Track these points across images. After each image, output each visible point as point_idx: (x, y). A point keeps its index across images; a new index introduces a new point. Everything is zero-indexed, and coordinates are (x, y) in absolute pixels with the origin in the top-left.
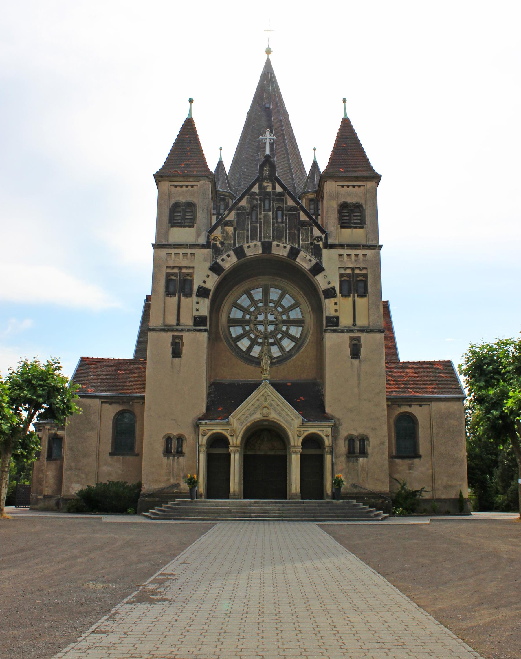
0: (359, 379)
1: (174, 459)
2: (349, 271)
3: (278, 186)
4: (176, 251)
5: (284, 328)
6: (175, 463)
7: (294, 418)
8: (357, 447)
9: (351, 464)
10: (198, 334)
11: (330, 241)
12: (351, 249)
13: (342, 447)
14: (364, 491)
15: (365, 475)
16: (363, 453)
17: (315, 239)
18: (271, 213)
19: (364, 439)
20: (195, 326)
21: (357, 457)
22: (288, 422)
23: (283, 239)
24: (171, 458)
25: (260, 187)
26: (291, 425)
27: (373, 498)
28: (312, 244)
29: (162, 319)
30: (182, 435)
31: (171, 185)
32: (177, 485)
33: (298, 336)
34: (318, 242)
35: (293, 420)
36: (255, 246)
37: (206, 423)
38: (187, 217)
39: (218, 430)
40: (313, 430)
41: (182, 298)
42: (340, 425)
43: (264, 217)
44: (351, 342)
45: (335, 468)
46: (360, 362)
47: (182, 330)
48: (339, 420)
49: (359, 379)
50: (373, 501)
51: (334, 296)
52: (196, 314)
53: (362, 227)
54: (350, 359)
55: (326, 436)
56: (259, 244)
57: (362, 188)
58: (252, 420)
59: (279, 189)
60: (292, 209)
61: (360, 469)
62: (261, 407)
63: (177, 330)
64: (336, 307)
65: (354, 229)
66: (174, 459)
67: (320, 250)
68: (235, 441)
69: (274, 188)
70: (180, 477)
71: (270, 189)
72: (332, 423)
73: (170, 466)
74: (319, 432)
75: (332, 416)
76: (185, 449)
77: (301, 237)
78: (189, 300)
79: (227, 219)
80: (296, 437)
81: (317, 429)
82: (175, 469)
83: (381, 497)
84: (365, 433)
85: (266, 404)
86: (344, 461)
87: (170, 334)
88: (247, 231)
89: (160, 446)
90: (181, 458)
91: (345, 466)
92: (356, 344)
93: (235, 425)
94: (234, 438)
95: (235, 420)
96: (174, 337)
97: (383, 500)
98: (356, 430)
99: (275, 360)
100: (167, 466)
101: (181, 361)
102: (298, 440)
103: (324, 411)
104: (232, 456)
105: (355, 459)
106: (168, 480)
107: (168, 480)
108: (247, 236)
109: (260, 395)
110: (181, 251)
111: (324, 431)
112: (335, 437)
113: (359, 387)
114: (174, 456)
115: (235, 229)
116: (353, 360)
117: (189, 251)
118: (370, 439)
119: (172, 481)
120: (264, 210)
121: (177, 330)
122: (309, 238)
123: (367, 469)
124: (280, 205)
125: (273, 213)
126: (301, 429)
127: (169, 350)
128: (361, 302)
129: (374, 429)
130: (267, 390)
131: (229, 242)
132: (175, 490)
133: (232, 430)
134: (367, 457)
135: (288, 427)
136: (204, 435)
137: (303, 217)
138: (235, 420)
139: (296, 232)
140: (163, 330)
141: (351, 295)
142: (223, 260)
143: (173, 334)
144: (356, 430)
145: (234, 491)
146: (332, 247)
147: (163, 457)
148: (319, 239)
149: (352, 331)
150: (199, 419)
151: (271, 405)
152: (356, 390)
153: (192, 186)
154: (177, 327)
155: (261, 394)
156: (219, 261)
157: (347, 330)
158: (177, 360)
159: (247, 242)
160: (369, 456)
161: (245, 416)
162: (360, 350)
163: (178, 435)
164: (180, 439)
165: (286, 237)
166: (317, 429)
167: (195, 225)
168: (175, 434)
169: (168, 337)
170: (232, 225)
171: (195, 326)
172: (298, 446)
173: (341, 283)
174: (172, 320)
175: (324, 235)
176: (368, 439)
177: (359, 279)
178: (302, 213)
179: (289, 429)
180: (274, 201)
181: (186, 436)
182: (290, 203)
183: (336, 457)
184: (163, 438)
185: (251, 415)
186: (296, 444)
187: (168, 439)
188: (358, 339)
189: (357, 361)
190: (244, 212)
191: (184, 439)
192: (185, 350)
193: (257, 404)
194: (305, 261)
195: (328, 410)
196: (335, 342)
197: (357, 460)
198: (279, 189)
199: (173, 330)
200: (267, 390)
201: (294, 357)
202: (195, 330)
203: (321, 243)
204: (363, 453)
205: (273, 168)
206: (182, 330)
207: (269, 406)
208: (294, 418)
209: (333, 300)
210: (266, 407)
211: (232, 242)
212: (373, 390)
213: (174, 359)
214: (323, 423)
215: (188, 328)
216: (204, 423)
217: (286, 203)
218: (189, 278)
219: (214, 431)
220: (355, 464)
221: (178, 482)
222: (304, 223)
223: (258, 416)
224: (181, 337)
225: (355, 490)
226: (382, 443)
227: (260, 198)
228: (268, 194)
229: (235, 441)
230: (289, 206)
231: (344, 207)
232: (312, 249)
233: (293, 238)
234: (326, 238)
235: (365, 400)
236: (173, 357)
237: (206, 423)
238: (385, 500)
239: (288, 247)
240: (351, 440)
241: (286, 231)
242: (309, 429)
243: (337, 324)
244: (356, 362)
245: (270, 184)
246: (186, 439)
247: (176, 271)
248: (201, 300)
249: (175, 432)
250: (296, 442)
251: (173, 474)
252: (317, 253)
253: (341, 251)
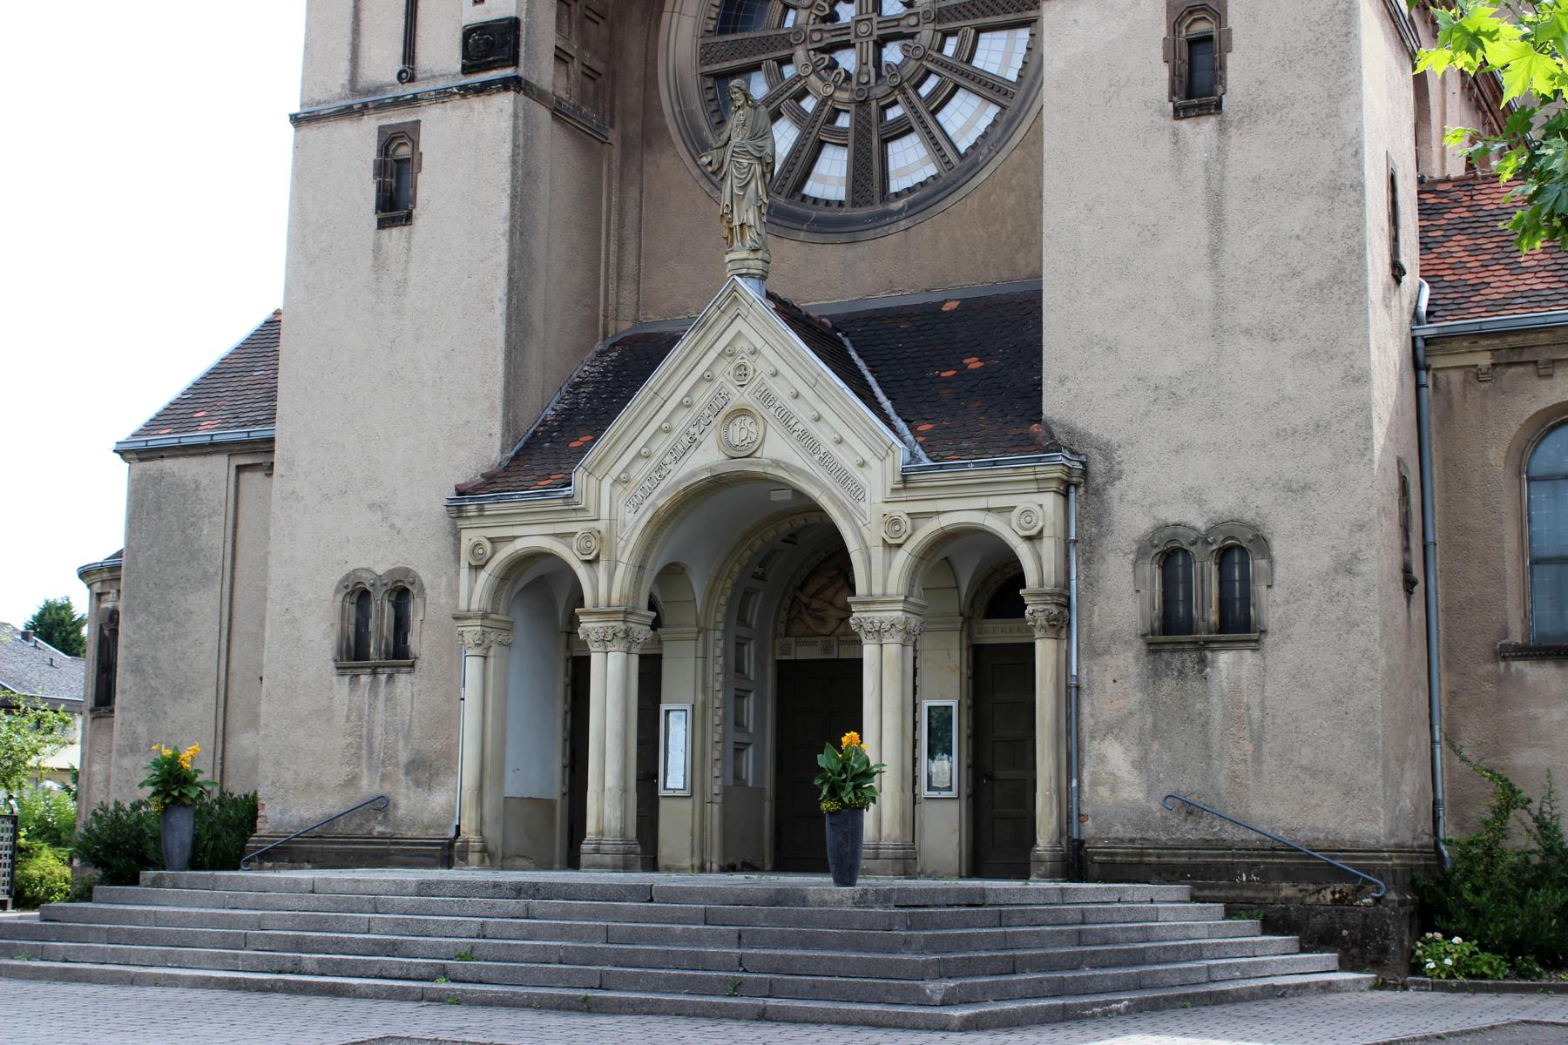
0: (1217, 220)
1: (374, 688)
6: (380, 706)
7: (867, 455)
8: (1208, 595)
9: (1168, 685)
10: (476, 103)
13: (1123, 597)
14: (1240, 835)
15: (1248, 747)
16: (1238, 624)
19: (1238, 552)
20: (466, 70)
21: (1202, 646)
22: (844, 478)
24: (365, 679)
26: (858, 492)
27: (1288, 874)
29: (344, 66)
30: (407, 571)
32: (380, 805)
33: (1012, 76)
35: (863, 464)
37: (481, 509)
39: (532, 537)
40: (960, 512)
42: (1113, 476)
44: (1175, 26)
45: (1086, 709)
46: (1222, 129)
47: (415, 100)
48: (1107, 450)
49: (1217, 220)
50: (1287, 890)
54: (1169, 122)
55: (1029, 538)
58: (679, 482)
61: (1217, 715)
62: (721, 416)
63: (398, 102)
66: (374, 688)
68: (607, 585)
70: (397, 765)
72: (1052, 470)
73: (360, 718)
74: (993, 523)
75: (1070, 432)
80: (878, 553)
81: (982, 503)
82: (378, 731)
83: (1340, 874)
84: (1249, 516)
85: (739, 398)
86: (1133, 669)
89: (320, 630)
90: (402, 680)
91: (1134, 698)
92: (1207, 39)
93: (605, 513)
94: (602, 568)
95: (607, 482)
96: (389, 140)
97: (1347, 887)
98: (1200, 502)
99: (900, 204)
100: (348, 718)
101: (409, 240)
102: (888, 567)
103: (1035, 413)
104: (596, 660)
105: (1190, 659)
106: (352, 781)
107: (352, 781)
109: (712, 355)
111: (1015, 509)
112: (1081, 544)
113: (1215, 264)
114: (374, 673)
116: (1184, 125)
118: (1278, 547)
119: (368, 787)
121: (398, 102)
123: (1256, 714)
126: (900, 510)
127: (366, 192)
129: (1296, 490)
130: (746, 330)
132: (379, 829)
133: (588, 536)
134: (1256, 644)
135: (842, 506)
136: (476, 568)
138: (607, 482)
140: (347, 112)
143: (385, 122)
144: (1200, 502)
145: (600, 833)
147: (334, 679)
150: (461, 491)
151: (767, 397)
152: (1201, 285)
154: (409, 90)
155: (719, 347)
158: (395, 234)
160: (1268, 640)
161: (653, 462)
162: (1223, 67)
163: (392, 572)
164: (401, 594)
166: (982, 503)
168: (380, 570)
172: (885, 600)
174: (382, 64)
176: (1261, 543)
179: (849, 516)
181: (426, 577)
183: (1092, 651)
184: (337, 591)
185: (679, 455)
186: (877, 590)
187: (359, 595)
189: (1208, 124)
191: (414, 590)
192: (429, 188)
193: (704, 395)
195: (1054, 403)
197: (1203, 662)
199: (381, 106)
200: (746, 330)
201: (984, 175)
202: (466, 91)
204: (1238, 624)
207: (756, 406)
208: (867, 455)
210: (742, 412)
212: (1295, 274)
213: (385, 233)
214: (1004, 472)
215: (440, 84)
216: (472, 509)
219: (520, 546)
220: (1194, 685)
221: (387, 789)
223: (707, 458)
224: (410, 134)
225: (1191, 831)
226: (1347, 566)
229: (607, 585)
235: (1247, 332)
236: (382, 224)
237: (481, 509)
238: (1359, 891)
240: (1170, 555)
244: (1200, 132)
246: (422, 589)
249: (379, 564)
250: (881, 575)
251: (371, 753)
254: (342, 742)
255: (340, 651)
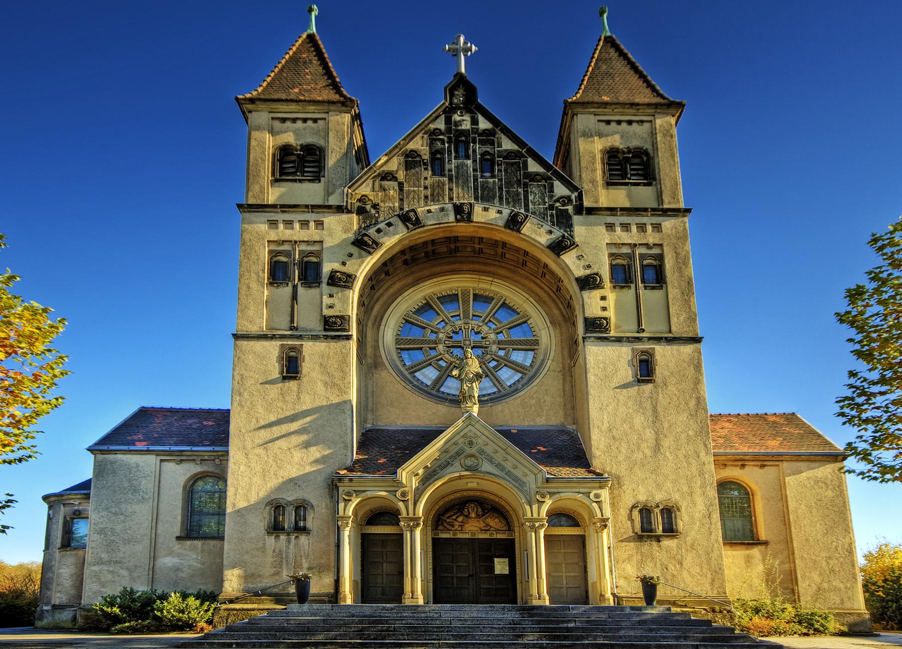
1: (289, 541)
2: (626, 250)
3: (481, 118)
4: (287, 217)
5: (502, 353)
11: (587, 203)
12: (630, 215)
17: (558, 200)
18: (469, 162)
20: (325, 330)
23: (497, 201)
25: (448, 121)
28: (551, 207)
31: (273, 118)
34: (563, 205)
36: (442, 210)
38: (306, 169)
41: (301, 290)
43: (457, 167)
46: (655, 387)
51: (599, 286)
52: (327, 312)
53: (649, 184)
56: (450, 207)
57: (647, 126)
59: (484, 124)
60: (509, 154)
64: (603, 304)
65: (633, 187)
67: (569, 218)
69: (475, 122)
71: (467, 125)
76: (311, 522)
77: (531, 198)
78: (314, 292)
79: (385, 168)
87: (279, 343)
88: (426, 188)
100: (274, 551)
108: (426, 197)
110: (296, 217)
114: (288, 534)
115: (401, 185)
117: (311, 217)
120: (456, 158)
122: (547, 200)
124: (489, 150)
125: (474, 161)
128: (651, 298)
131: (391, 205)
137: (533, 167)
139: (521, 190)
141: (633, 286)
142: (379, 231)
146: (591, 211)
148: (567, 200)
149: (639, 339)
153: (315, 121)
156: (372, 231)
157: (628, 338)
159: (426, 205)
164: (301, 507)
165: (501, 198)
167: (322, 179)
168: (290, 499)
169: (273, 348)
170: (395, 179)
171: (325, 330)
173: (613, 267)
175: (576, 194)
177: (645, 262)
178: (530, 161)
180: (475, 143)
182: (507, 145)
188: (650, 354)
189: (650, 386)
190: (418, 159)
194: (537, 234)
196: (606, 363)
198: (484, 124)
199: (283, 337)
202: (326, 337)
203: (570, 208)
204: (670, 530)
205: (471, 92)
206: (300, 337)
209: (597, 293)
211: (397, 204)
217: (500, 145)
218: (314, 259)
222: (533, 177)
227: (449, 138)
228: (465, 133)
230: (506, 150)
231: (612, 154)
232: (552, 215)
233: (514, 199)
234: (580, 197)
239: (506, 212)
241: (501, 189)
242: (560, 490)
243: (606, 330)
245: (467, 118)
247: (286, 247)
248: (334, 290)
252: (563, 220)
253: (610, 219)
254: (272, 560)
255: (268, 527)
